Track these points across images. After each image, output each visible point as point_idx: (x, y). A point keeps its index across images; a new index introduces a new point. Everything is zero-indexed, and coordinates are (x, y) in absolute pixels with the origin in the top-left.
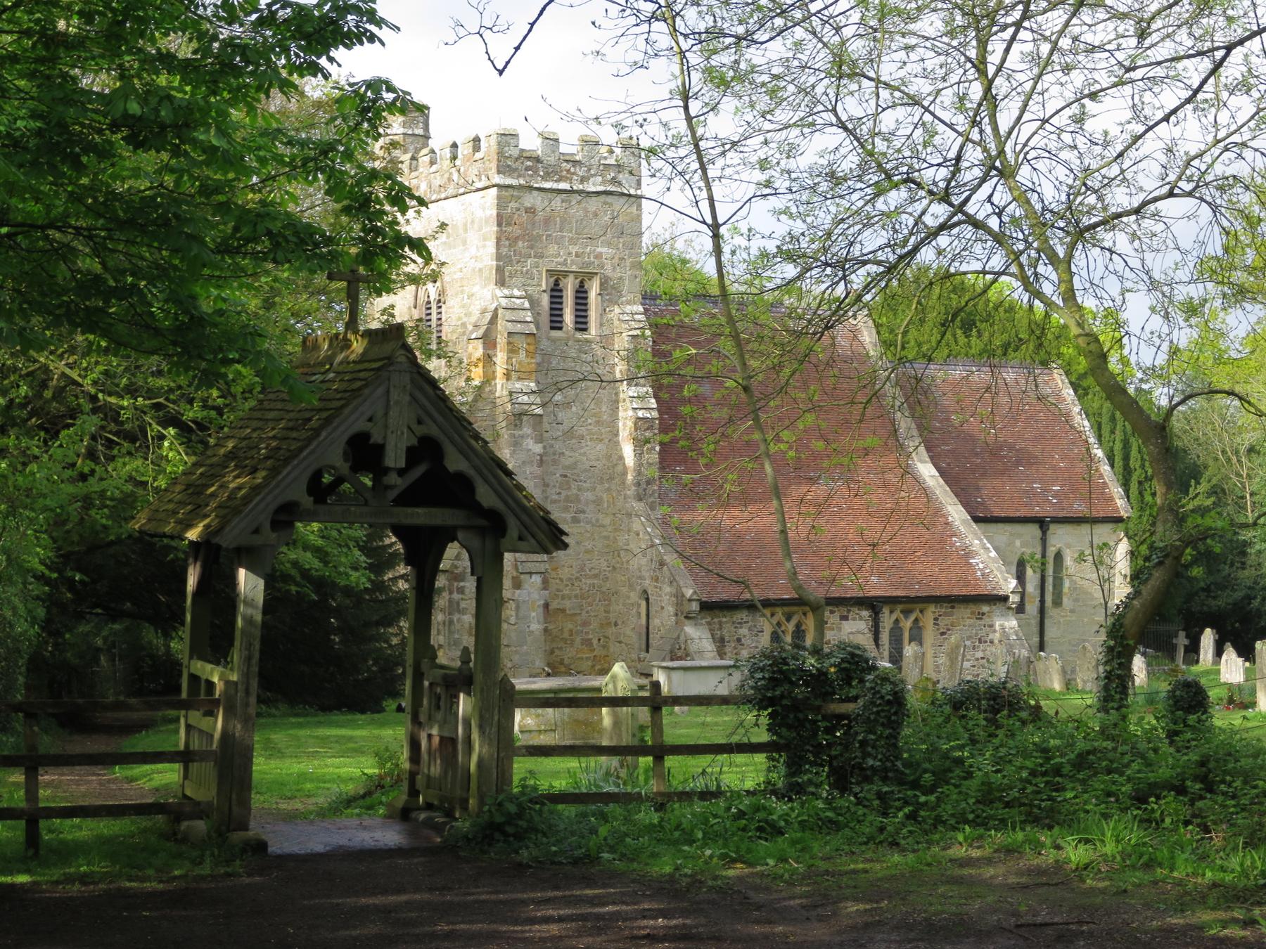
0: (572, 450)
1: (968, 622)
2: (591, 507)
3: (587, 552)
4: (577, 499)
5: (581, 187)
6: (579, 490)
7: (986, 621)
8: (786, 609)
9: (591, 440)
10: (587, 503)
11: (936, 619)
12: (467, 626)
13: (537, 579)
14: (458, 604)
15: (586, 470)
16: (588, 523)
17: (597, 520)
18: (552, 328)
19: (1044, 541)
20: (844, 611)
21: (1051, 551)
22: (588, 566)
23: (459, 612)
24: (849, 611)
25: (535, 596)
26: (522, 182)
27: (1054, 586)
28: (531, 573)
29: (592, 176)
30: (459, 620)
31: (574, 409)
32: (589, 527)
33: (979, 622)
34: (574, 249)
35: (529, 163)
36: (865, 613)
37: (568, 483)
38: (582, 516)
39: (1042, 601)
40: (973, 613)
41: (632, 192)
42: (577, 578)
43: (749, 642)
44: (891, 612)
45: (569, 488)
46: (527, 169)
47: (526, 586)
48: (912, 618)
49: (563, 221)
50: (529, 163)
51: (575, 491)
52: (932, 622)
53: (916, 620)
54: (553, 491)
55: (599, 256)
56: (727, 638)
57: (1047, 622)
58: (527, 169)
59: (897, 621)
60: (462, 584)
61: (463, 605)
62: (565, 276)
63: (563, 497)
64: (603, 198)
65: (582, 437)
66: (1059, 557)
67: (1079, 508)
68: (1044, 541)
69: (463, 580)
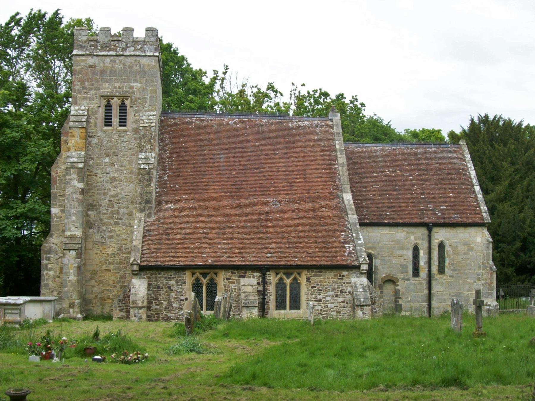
0: (115, 187)
1: (332, 280)
2: (126, 216)
3: (124, 240)
4: (118, 213)
5: (121, 53)
6: (119, 208)
7: (345, 280)
8: (202, 271)
9: (126, 182)
10: (123, 215)
11: (308, 279)
12: (51, 277)
13: (73, 253)
14: (46, 266)
15: (123, 198)
16: (124, 225)
17: (130, 224)
18: (106, 125)
19: (430, 236)
20: (242, 272)
21: (435, 243)
22: (124, 247)
23: (47, 270)
24: (245, 273)
25: (72, 261)
26: (88, 52)
27: (439, 262)
28: (70, 250)
29: (128, 47)
30: (47, 274)
31: (116, 166)
32: (124, 227)
33: (340, 281)
34: (117, 85)
35: (92, 43)
36: (257, 274)
37: (112, 204)
38: (120, 221)
39: (430, 271)
40: (334, 276)
41: (151, 54)
42: (117, 254)
43: (176, 289)
44: (277, 274)
45: (113, 207)
46: (91, 46)
47: (67, 256)
48: (292, 277)
49: (111, 71)
50: (92, 43)
51: (116, 209)
52: (305, 280)
53: (295, 279)
54: (104, 209)
55: (131, 88)
56: (161, 286)
57: (434, 283)
58: (91, 46)
59: (281, 279)
60: (49, 255)
61: (49, 266)
62: (113, 99)
63: (109, 211)
64: (134, 58)
65: (121, 181)
66: (441, 246)
67: (455, 218)
68: (430, 236)
69: (49, 254)
